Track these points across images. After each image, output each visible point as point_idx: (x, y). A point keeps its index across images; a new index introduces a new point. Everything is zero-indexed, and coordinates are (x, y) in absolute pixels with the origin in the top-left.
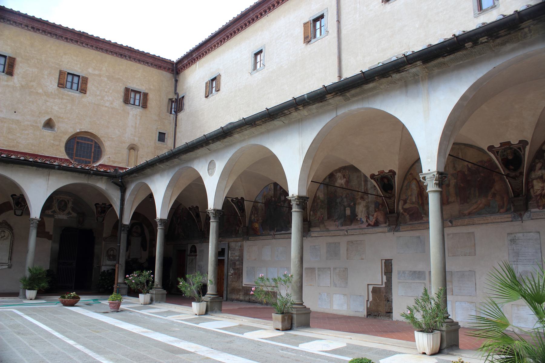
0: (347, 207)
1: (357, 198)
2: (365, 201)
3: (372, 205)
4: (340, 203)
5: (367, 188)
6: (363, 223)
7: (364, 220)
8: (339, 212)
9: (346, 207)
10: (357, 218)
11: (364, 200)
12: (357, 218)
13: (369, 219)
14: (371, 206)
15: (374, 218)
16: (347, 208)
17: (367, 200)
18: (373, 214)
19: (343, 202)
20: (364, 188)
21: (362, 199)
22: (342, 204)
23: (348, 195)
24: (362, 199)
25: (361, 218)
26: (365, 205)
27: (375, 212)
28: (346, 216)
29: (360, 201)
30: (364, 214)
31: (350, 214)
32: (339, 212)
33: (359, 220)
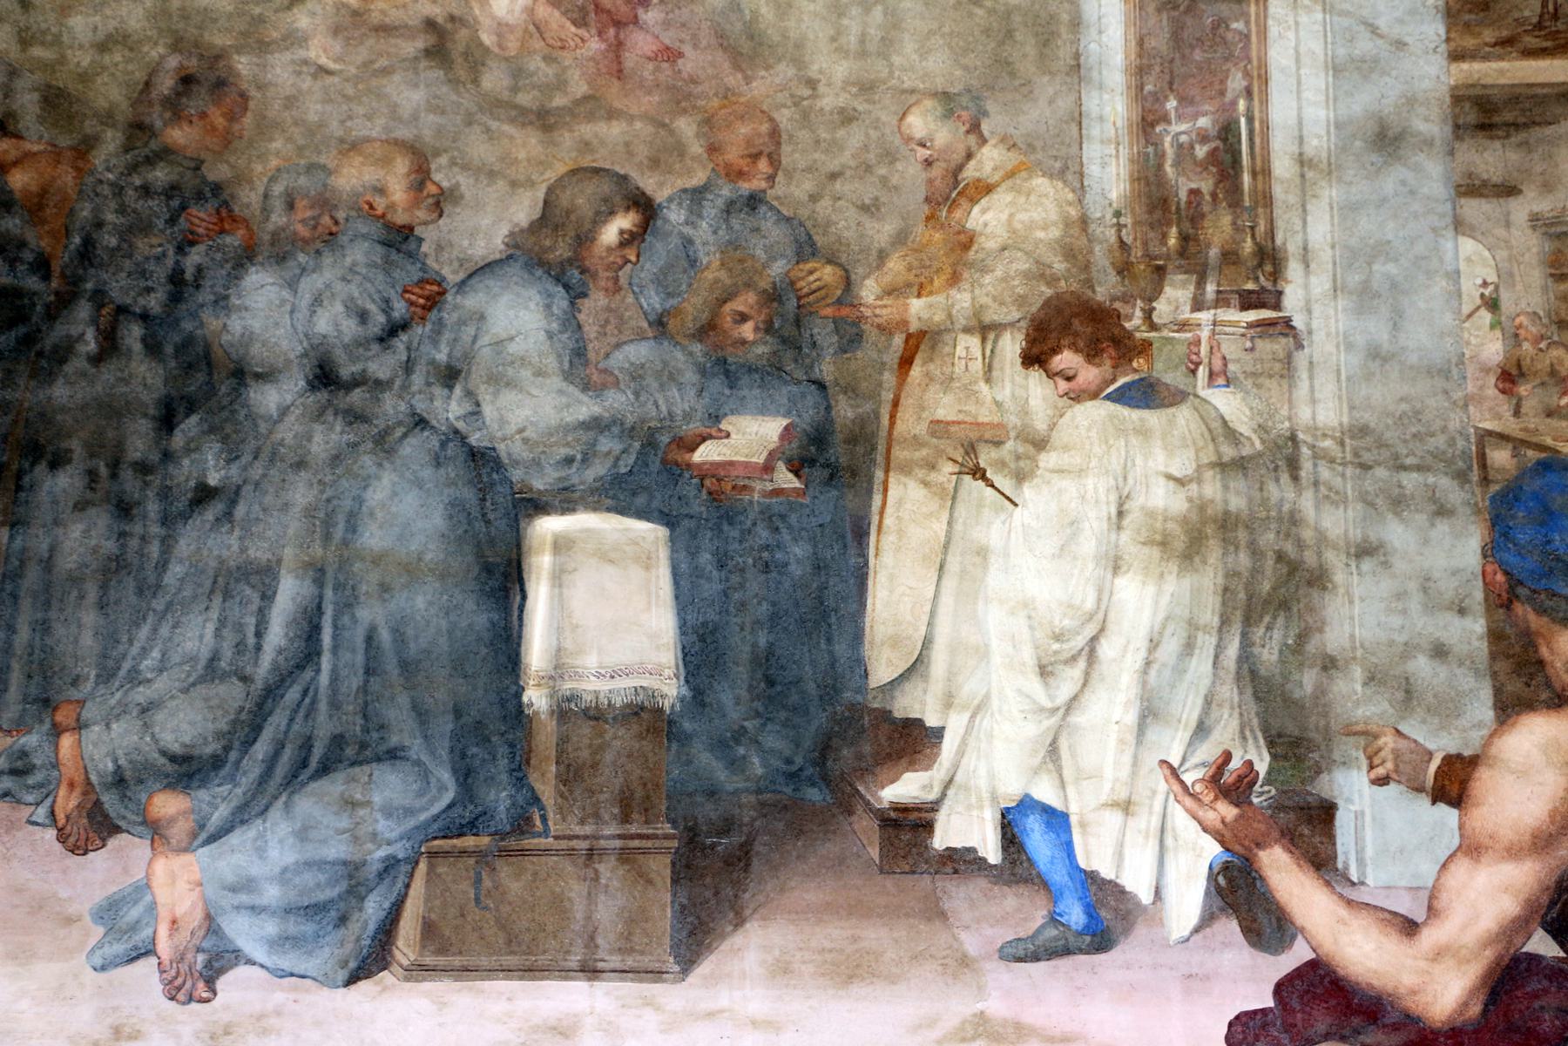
0: (565, 500)
1: (918, 309)
2: (1183, 416)
3: (1397, 534)
4: (324, 377)
5: (1227, 132)
6: (1099, 939)
7: (1138, 883)
8: (290, 592)
9: (538, 506)
10: (905, 788)
11: (1145, 394)
12: (905, 788)
13: (1321, 862)
14: (1364, 551)
15: (1471, 848)
16: (548, 526)
17: (1225, 402)
18: (1442, 743)
19: (450, 375)
20: (1147, 123)
21: (1066, 359)
22: (421, 422)
23: (610, 233)
24: (1066, 359)
25: (1057, 820)
26: (1162, 499)
27: (1509, 708)
28: (516, 716)
29: (1037, 390)
30: (1150, 713)
31: (670, 689)
32: (290, 592)
33: (961, 862)
